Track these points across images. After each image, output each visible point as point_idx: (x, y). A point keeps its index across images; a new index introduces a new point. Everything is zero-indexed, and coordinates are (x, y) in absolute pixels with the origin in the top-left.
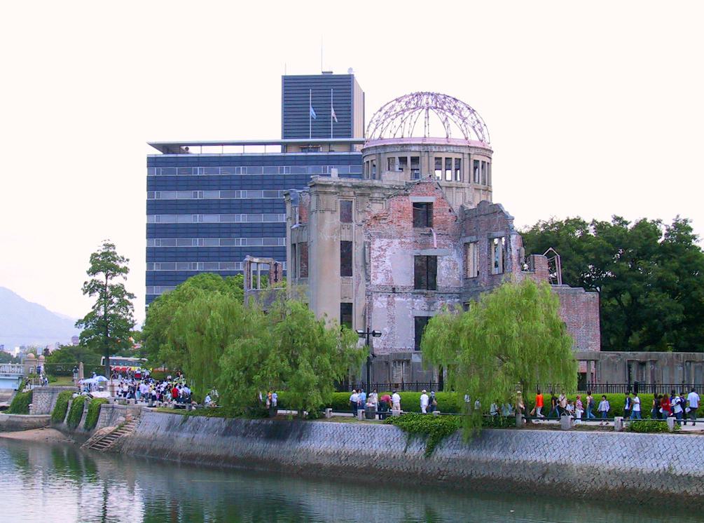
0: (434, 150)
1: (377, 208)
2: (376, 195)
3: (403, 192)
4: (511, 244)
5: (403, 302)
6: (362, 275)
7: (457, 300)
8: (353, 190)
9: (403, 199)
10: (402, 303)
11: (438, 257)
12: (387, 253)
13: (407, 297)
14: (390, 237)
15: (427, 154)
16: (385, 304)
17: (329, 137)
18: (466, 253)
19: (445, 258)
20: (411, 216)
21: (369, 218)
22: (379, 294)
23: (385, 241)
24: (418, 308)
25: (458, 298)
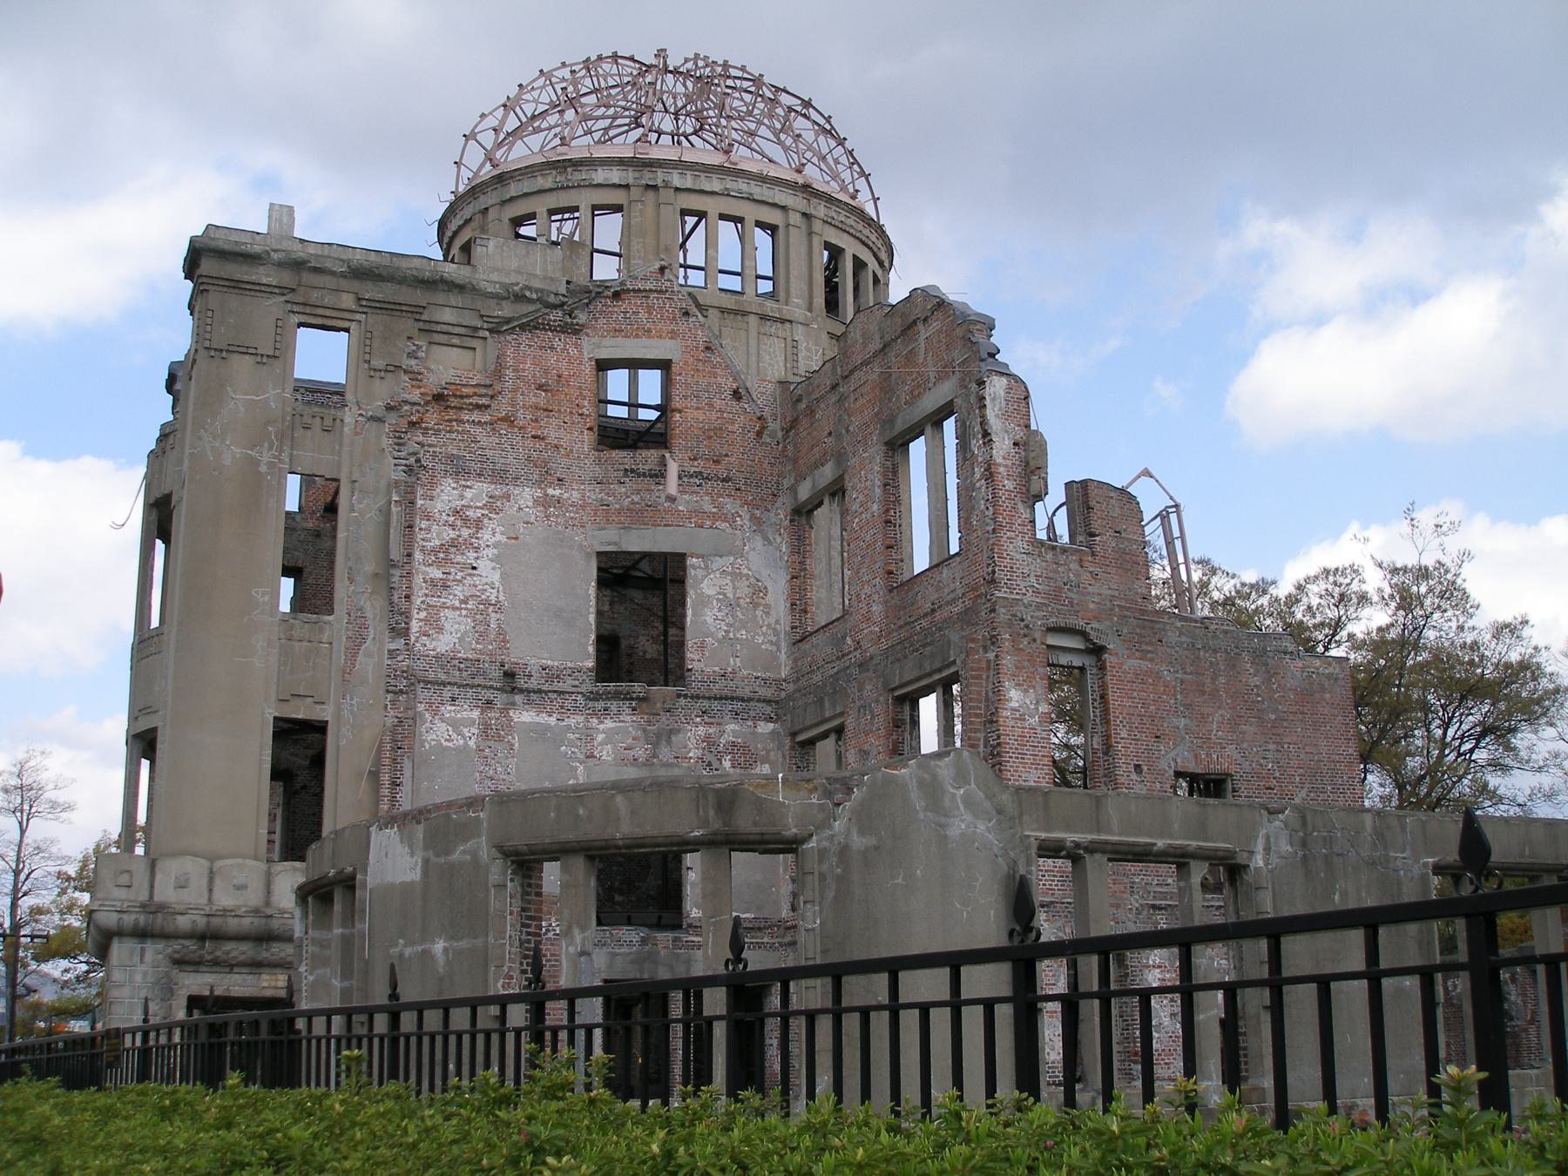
0: (677, 181)
2: (448, 316)
3: (556, 316)
4: (990, 413)
5: (548, 727)
6: (373, 609)
7: (765, 728)
8: (356, 285)
10: (540, 731)
12: (486, 535)
14: (499, 476)
15: (651, 195)
18: (800, 546)
19: (718, 563)
21: (415, 396)
22: (447, 694)
23: (478, 492)
24: (606, 753)
25: (769, 719)
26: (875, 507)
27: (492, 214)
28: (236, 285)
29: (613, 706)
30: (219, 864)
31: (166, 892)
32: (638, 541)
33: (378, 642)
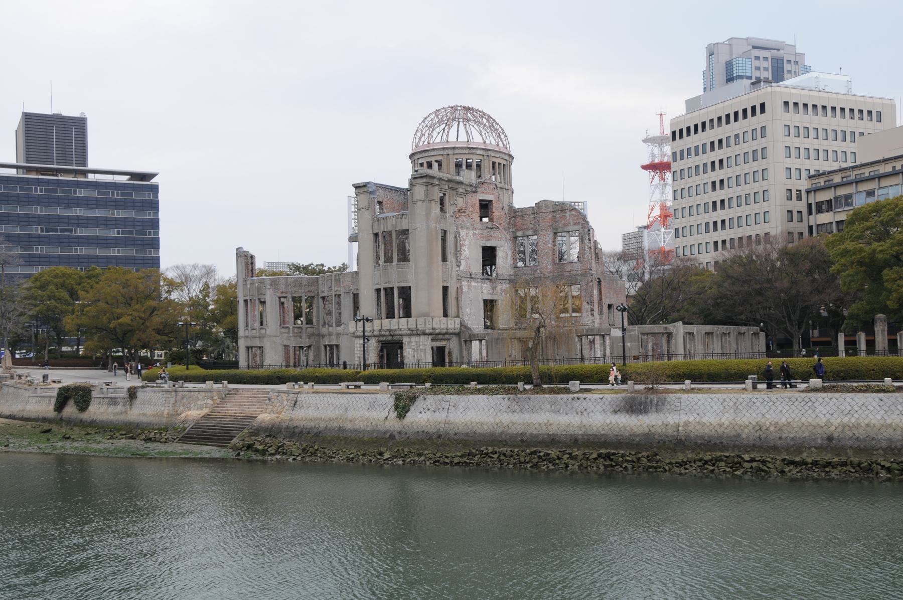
0: (493, 154)
1: (460, 202)
2: (460, 190)
6: (454, 260)
7: (508, 285)
9: (473, 194)
10: (475, 287)
11: (498, 248)
13: (478, 282)
14: (467, 229)
16: (466, 287)
17: (71, 164)
19: (502, 249)
20: (479, 212)
21: (456, 210)
26: (550, 245)
27: (451, 156)
28: (432, 184)
29: (486, 281)
30: (441, 319)
31: (435, 326)
32: (489, 244)
33: (455, 268)
